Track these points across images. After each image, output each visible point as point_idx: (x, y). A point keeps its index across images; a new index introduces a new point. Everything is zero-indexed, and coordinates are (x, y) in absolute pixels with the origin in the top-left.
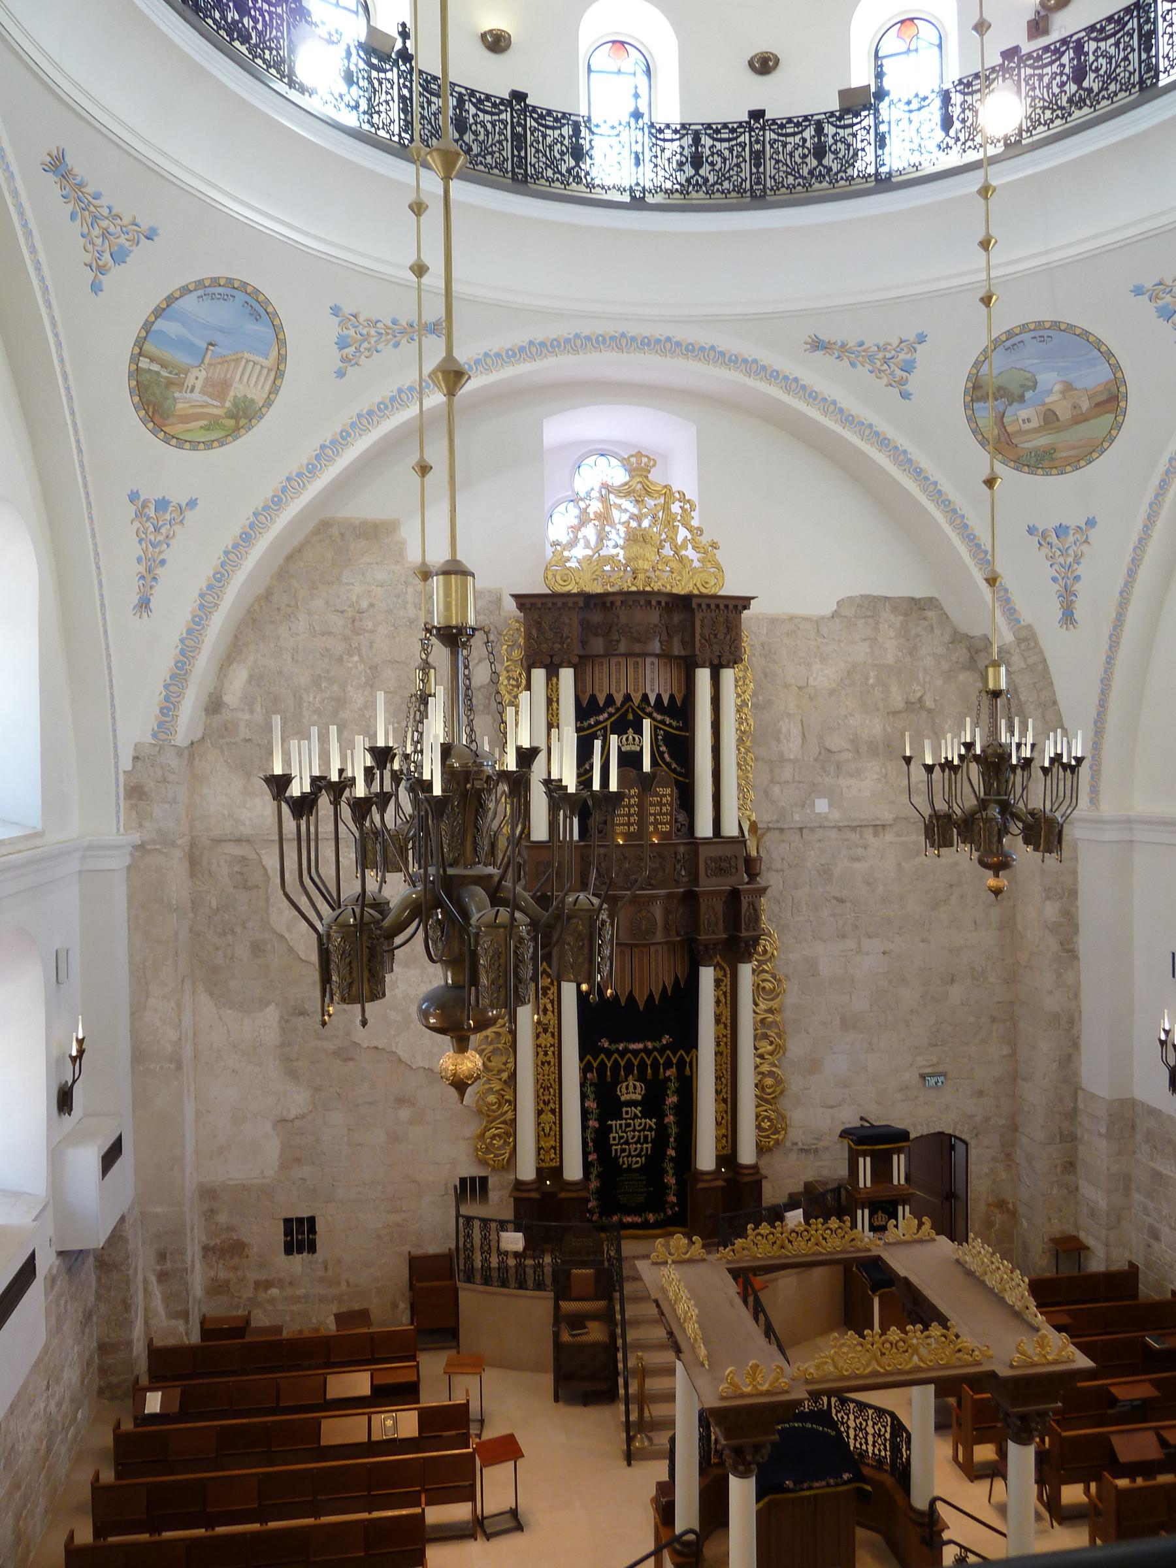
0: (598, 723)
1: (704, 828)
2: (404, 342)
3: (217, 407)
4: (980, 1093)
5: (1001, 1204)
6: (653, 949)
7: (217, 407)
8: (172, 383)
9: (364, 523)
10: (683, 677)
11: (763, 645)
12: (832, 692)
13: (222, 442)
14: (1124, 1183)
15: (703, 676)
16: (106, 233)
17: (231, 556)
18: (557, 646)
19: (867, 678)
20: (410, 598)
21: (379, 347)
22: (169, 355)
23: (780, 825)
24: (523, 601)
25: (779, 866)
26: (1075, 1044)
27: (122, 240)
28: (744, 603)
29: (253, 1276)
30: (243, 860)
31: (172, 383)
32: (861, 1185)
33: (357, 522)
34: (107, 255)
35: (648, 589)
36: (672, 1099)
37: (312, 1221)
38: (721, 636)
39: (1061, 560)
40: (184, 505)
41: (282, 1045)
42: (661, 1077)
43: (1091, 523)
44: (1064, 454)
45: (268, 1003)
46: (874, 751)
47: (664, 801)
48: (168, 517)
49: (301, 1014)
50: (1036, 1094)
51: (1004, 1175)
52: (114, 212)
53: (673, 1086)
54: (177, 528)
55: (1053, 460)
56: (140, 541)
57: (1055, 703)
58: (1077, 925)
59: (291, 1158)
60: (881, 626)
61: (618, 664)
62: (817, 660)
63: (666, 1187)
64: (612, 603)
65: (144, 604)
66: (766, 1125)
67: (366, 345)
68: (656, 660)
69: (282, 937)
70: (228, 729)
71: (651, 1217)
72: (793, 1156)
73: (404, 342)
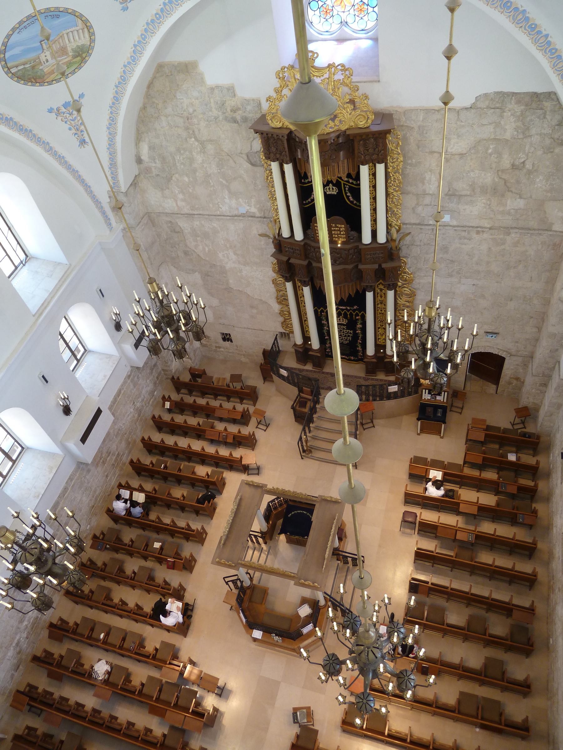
1: (367, 238)
3: (66, 58)
4: (517, 342)
5: (517, 379)
7: (66, 58)
9: (180, 64)
11: (419, 127)
12: (462, 155)
13: (79, 67)
19: (487, 149)
20: (213, 105)
22: (23, 60)
25: (419, 243)
29: (214, 345)
30: (171, 222)
36: (359, 326)
42: (354, 319)
45: (195, 272)
46: (484, 190)
51: (521, 370)
53: (360, 322)
56: (66, 122)
60: (505, 114)
62: (456, 137)
63: (358, 351)
70: (148, 170)
71: (352, 358)
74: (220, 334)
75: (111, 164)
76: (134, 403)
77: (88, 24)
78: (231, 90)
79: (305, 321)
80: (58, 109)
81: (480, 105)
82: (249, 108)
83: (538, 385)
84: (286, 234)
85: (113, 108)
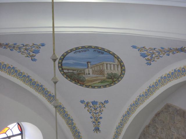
2: (171, 54)
7: (102, 77)
8: (80, 74)
9: (180, 110)
13: (110, 85)
16: (26, 49)
21: (161, 55)
27: (33, 49)
31: (80, 74)
33: (178, 109)
34: (31, 53)
40: (103, 103)
48: (98, 105)
52: (25, 44)
54: (103, 108)
56: (90, 113)
65: (97, 129)
67: (154, 56)
73: (171, 54)
77: (122, 64)
85: (124, 118)
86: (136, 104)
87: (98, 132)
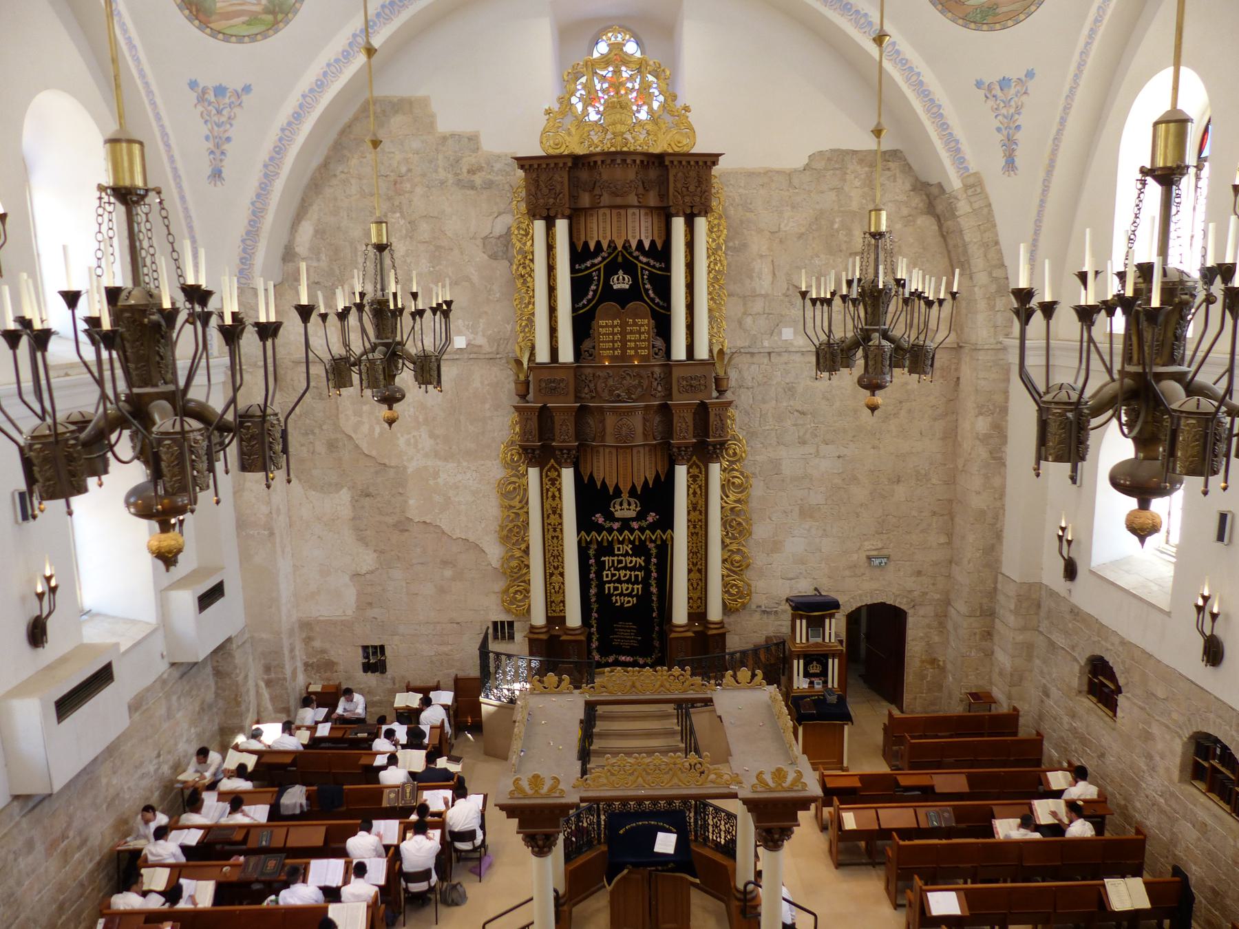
0: (593, 265)
1: (679, 353)
4: (919, 573)
5: (933, 661)
6: (635, 450)
10: (663, 225)
12: (800, 236)
13: (264, 35)
14: (1028, 650)
15: (679, 224)
17: (287, 133)
18: (551, 201)
19: (833, 223)
20: (440, 162)
23: (751, 350)
24: (523, 162)
26: (999, 536)
28: (713, 159)
32: (798, 641)
35: (625, 149)
37: (382, 647)
38: (692, 188)
39: (1004, 111)
41: (354, 519)
43: (1030, 74)
44: (1004, 9)
47: (643, 329)
49: (367, 495)
50: (964, 576)
51: (936, 639)
54: (237, 110)
55: (996, 15)
56: (206, 122)
57: (997, 243)
58: (1006, 437)
59: (365, 603)
60: (848, 177)
61: (605, 214)
64: (595, 162)
65: (217, 174)
66: (734, 591)
68: (637, 211)
69: (350, 438)
72: (757, 616)
74: (360, 651)
75: (248, 233)
76: (159, 756)
78: (473, 139)
79: (552, 575)
80: (204, 91)
81: (816, 165)
82: (497, 166)
83: (978, 637)
84: (543, 356)
86: (320, 85)
87: (219, 183)
